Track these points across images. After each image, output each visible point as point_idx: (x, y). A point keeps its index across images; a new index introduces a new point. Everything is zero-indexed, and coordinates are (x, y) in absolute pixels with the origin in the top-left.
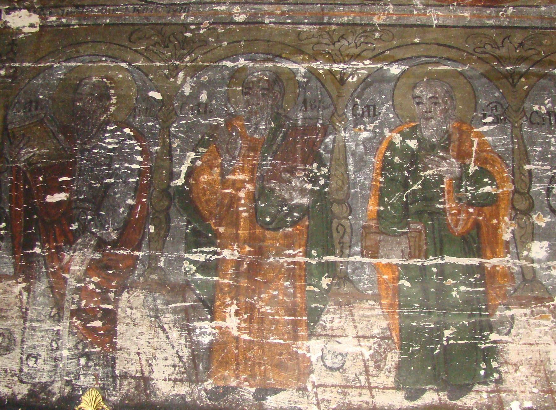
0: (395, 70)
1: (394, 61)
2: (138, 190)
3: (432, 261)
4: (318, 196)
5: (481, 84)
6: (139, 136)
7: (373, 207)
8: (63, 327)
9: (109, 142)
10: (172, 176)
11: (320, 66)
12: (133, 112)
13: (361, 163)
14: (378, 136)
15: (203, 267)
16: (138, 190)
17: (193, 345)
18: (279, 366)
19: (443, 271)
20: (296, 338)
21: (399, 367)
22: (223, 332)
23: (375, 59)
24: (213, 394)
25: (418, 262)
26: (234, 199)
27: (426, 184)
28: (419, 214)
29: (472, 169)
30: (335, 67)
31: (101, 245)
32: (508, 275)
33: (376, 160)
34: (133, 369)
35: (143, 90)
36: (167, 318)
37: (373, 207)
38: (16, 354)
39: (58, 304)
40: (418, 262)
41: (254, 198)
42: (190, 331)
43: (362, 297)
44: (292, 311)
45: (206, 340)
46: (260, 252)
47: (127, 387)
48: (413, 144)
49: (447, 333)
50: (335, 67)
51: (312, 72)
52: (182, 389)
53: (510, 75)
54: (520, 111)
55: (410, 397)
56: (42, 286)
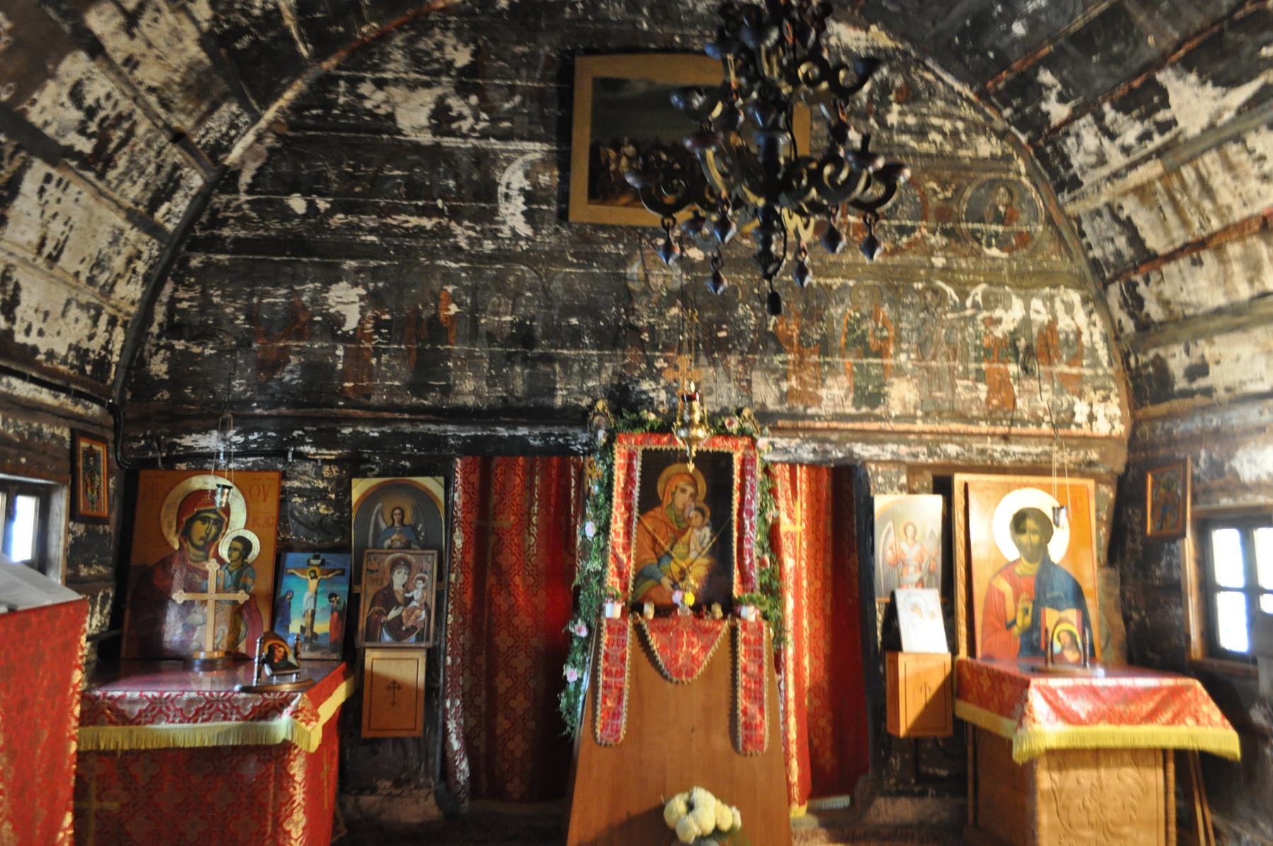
0: (851, 283)
1: (850, 278)
2: (754, 332)
3: (865, 361)
4: (823, 336)
5: (884, 290)
6: (753, 308)
7: (843, 340)
8: (731, 385)
9: (741, 311)
10: (767, 326)
11: (822, 281)
12: (749, 299)
13: (839, 322)
14: (845, 312)
15: (782, 363)
16: (754, 332)
17: (781, 391)
18: (812, 399)
19: (868, 365)
20: (817, 387)
21: (854, 400)
22: (791, 387)
23: (844, 277)
24: (789, 409)
25: (859, 361)
26: (792, 337)
27: (863, 332)
28: (860, 343)
29: (880, 325)
30: (829, 281)
31: (742, 353)
32: (892, 367)
33: (844, 322)
34: (760, 400)
35: (752, 290)
36: (771, 382)
37: (843, 340)
38: (714, 396)
39: (729, 376)
40: (859, 361)
41: (799, 336)
42: (779, 387)
43: (839, 374)
44: (816, 378)
45: (785, 389)
46: (802, 357)
47: (757, 407)
48: (858, 315)
49: (870, 387)
50: (829, 281)
51: (819, 284)
52: (777, 408)
53: (897, 288)
54: (899, 302)
55: (858, 408)
56: (721, 369)
